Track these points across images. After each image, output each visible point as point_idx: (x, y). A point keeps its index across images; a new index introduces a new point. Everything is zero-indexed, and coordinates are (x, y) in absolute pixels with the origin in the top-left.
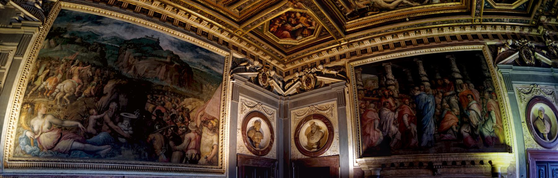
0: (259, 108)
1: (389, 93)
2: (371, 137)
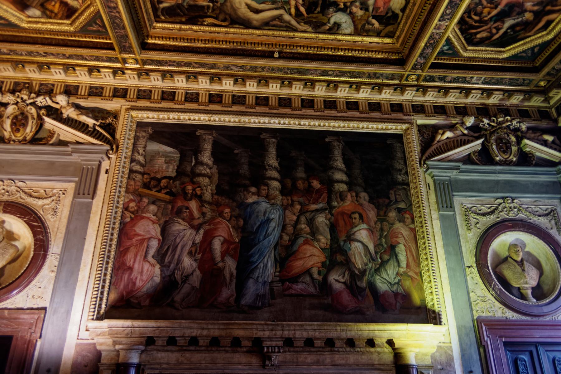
1: (194, 190)
2: (135, 274)
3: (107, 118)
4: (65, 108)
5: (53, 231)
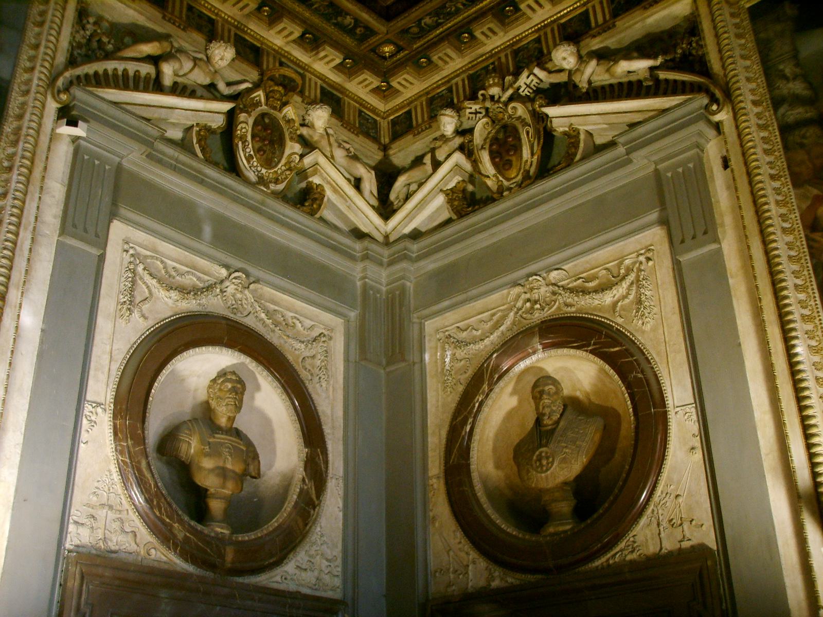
0: (233, 296)
3: (675, 46)
4: (577, 70)
5: (658, 354)
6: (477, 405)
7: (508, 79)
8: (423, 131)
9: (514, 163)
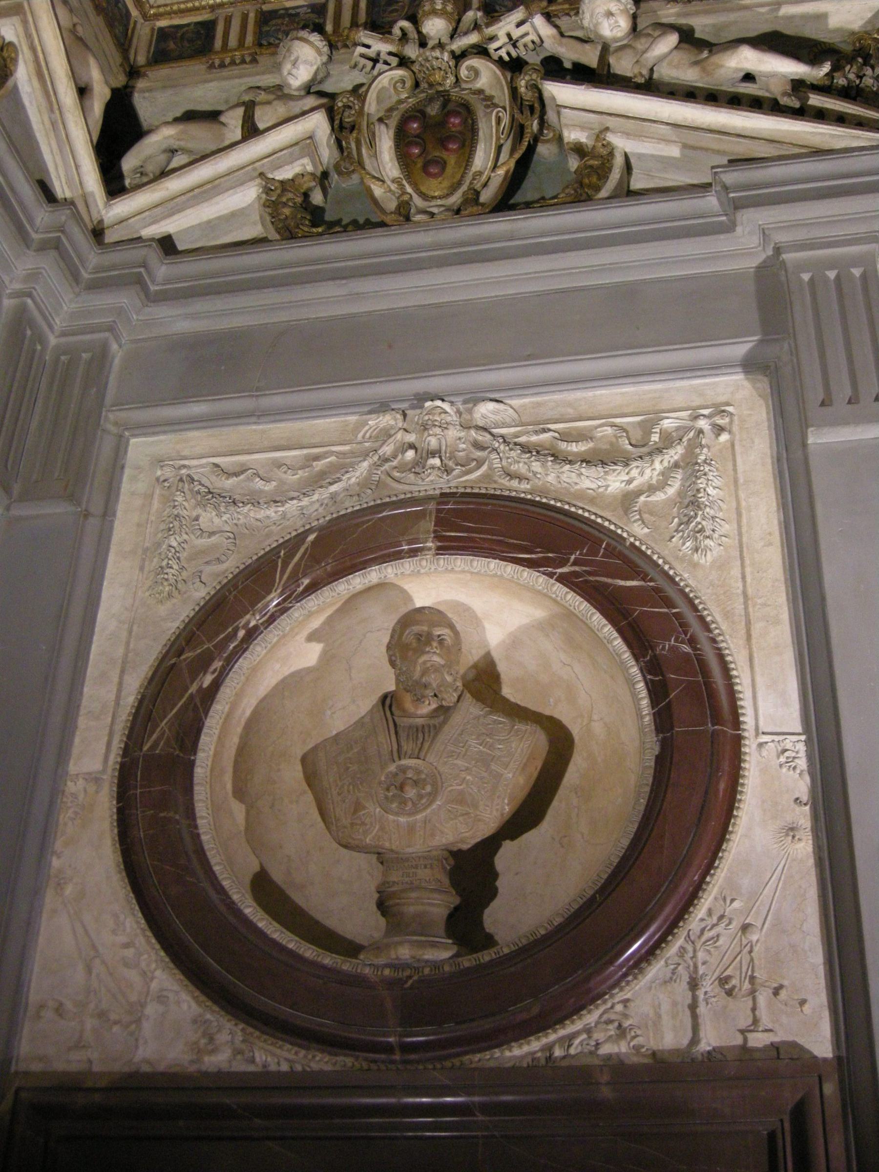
5: (727, 615)
6: (241, 633)
7: (470, 15)
8: (233, 63)
9: (449, 170)
